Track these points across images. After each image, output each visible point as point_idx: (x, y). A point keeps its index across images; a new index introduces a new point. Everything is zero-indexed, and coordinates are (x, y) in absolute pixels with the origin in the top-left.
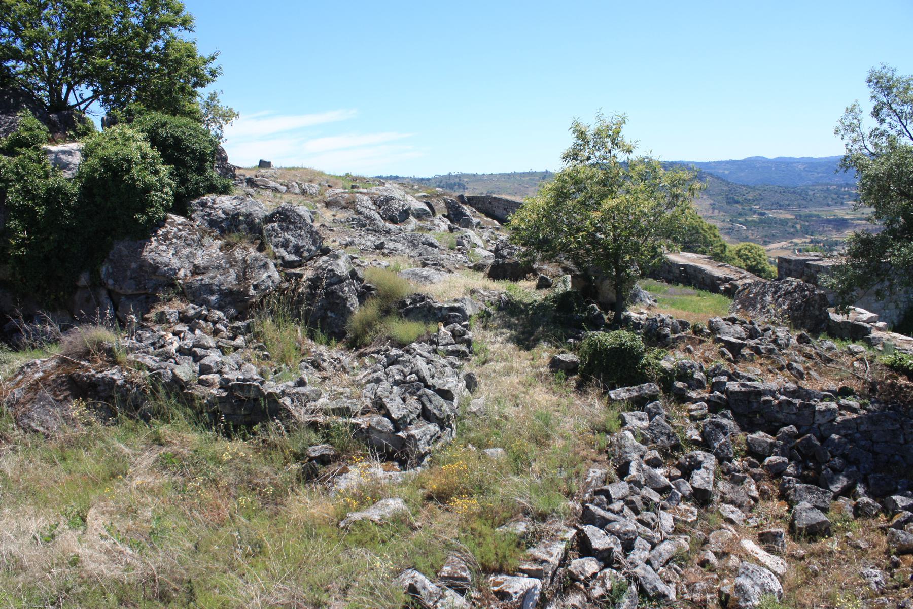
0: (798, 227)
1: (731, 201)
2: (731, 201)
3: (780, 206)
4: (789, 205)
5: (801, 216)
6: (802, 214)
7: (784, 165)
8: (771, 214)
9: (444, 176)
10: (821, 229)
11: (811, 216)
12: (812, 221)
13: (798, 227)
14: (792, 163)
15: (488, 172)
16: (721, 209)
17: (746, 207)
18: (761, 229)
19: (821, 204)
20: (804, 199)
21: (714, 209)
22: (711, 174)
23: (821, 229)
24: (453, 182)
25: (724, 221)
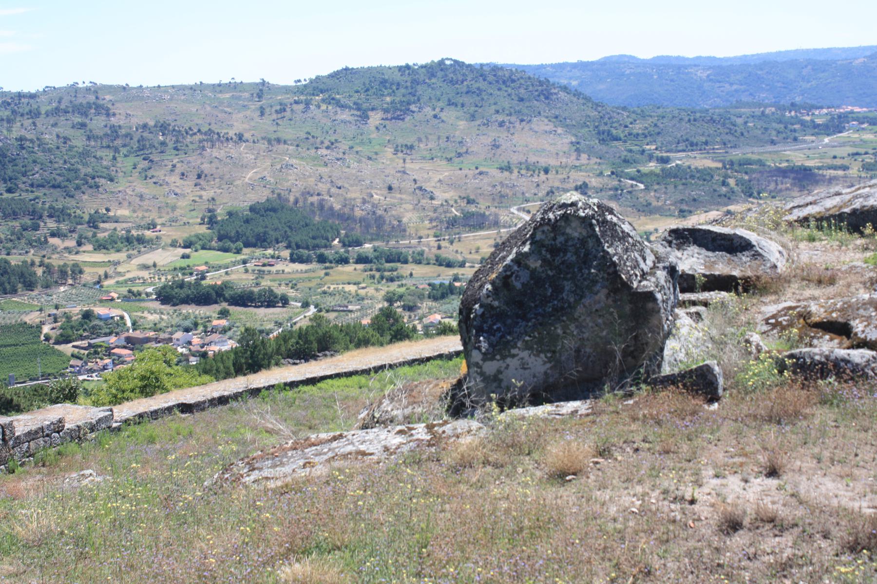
1: (607, 137)
2: (607, 137)
3: (692, 145)
4: (706, 143)
5: (732, 163)
6: (734, 158)
7: (671, 70)
8: (679, 160)
10: (772, 186)
11: (749, 162)
12: (753, 171)
14: (686, 67)
16: (590, 151)
17: (634, 148)
18: (671, 188)
19: (760, 142)
20: (730, 133)
22: (565, 89)
23: (772, 186)
25: (601, 174)
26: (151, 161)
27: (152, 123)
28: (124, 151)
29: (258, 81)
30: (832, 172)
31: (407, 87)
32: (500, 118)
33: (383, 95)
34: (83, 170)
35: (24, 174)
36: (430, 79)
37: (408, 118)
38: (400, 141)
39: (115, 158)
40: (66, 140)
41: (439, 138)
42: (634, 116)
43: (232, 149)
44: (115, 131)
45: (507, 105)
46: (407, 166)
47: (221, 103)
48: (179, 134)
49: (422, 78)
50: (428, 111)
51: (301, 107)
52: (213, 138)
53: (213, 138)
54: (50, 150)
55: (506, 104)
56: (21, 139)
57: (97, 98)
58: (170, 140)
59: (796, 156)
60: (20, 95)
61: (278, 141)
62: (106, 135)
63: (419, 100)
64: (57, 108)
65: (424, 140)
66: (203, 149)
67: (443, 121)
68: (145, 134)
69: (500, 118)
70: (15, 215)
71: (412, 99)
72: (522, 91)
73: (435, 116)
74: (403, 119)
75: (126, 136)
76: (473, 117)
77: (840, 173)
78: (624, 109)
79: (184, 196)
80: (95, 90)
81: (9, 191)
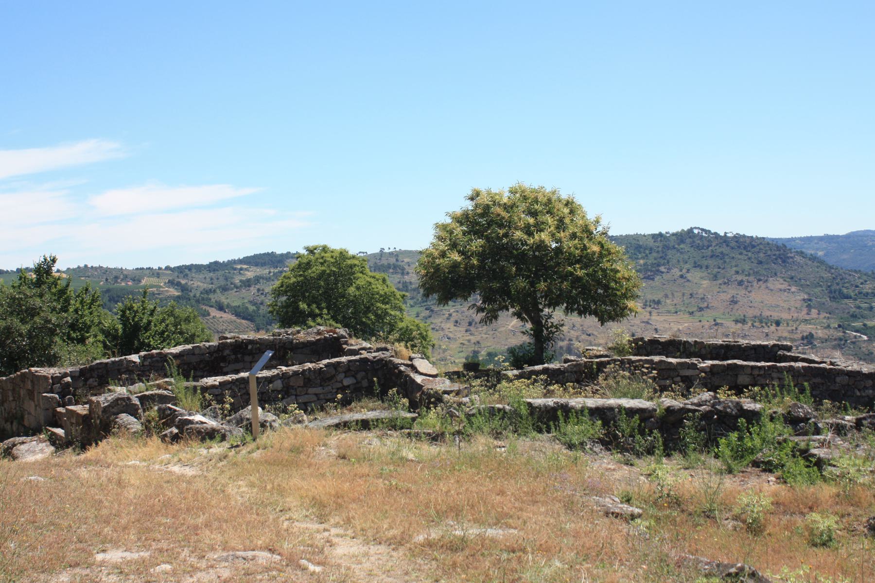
1: (837, 295)
2: (837, 295)
9: (374, 255)
17: (863, 305)
21: (809, 307)
26: (432, 311)
28: (412, 302)
31: (658, 252)
32: (739, 278)
33: (637, 259)
36: (679, 245)
37: (657, 278)
38: (649, 297)
41: (683, 295)
42: (865, 278)
45: (747, 267)
46: (655, 317)
49: (671, 244)
50: (676, 272)
55: (747, 266)
57: (397, 260)
63: (668, 262)
65: (670, 296)
67: (688, 281)
69: (739, 278)
71: (662, 261)
72: (761, 255)
73: (682, 276)
74: (653, 279)
76: (715, 277)
78: (856, 271)
79: (455, 339)
80: (396, 255)
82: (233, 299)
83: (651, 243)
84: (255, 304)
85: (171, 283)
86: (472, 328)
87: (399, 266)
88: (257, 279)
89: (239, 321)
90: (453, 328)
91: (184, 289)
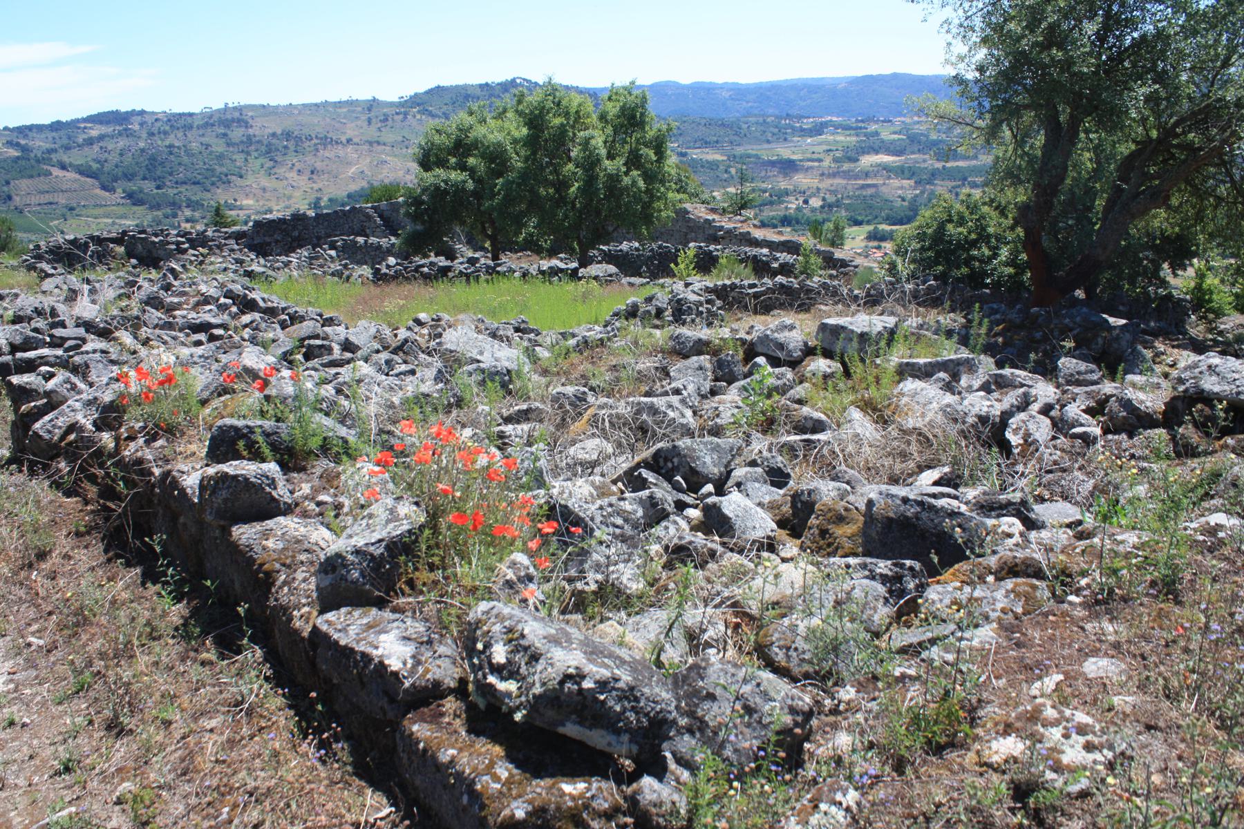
0: (733, 171)
3: (706, 144)
8: (695, 154)
9: (218, 111)
11: (749, 156)
13: (733, 171)
15: (284, 102)
19: (758, 141)
24: (229, 117)
27: (279, 132)
28: (256, 154)
29: (370, 98)
30: (810, 164)
34: (219, 169)
35: (171, 174)
39: (246, 160)
40: (207, 146)
43: (340, 151)
44: (249, 140)
47: (339, 116)
48: (298, 140)
51: (401, 117)
52: (326, 141)
53: (326, 141)
54: (193, 155)
56: (171, 146)
58: (291, 144)
59: (785, 152)
60: (181, 115)
61: (378, 143)
62: (242, 142)
64: (207, 123)
66: (317, 150)
68: (274, 141)
70: (158, 207)
75: (258, 142)
77: (816, 164)
80: (240, 109)
81: (158, 188)
82: (76, 157)
83: (478, 92)
84: (99, 162)
85: (10, 144)
86: (314, 177)
87: (243, 120)
88: (101, 138)
89: (83, 179)
90: (296, 177)
91: (25, 149)
